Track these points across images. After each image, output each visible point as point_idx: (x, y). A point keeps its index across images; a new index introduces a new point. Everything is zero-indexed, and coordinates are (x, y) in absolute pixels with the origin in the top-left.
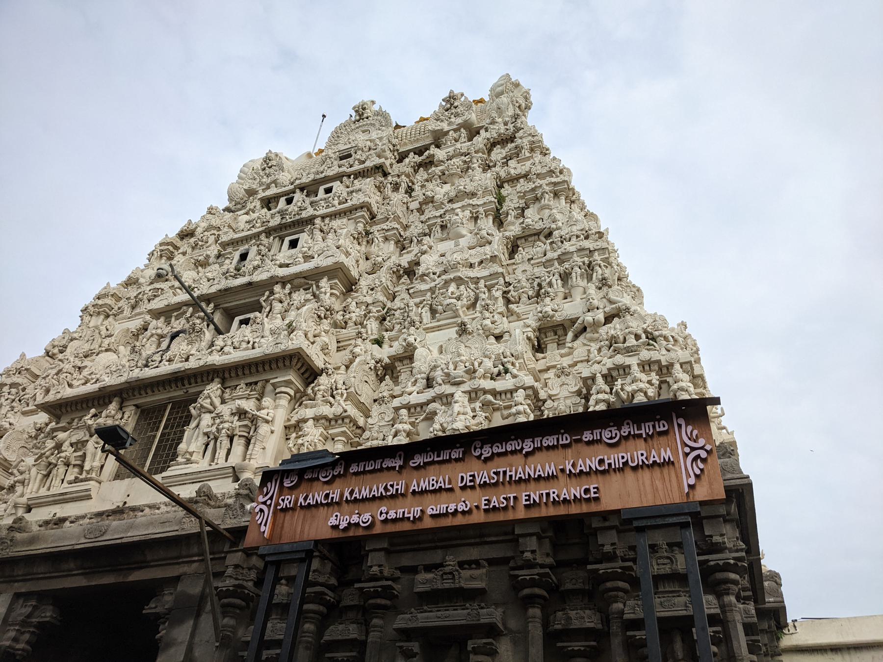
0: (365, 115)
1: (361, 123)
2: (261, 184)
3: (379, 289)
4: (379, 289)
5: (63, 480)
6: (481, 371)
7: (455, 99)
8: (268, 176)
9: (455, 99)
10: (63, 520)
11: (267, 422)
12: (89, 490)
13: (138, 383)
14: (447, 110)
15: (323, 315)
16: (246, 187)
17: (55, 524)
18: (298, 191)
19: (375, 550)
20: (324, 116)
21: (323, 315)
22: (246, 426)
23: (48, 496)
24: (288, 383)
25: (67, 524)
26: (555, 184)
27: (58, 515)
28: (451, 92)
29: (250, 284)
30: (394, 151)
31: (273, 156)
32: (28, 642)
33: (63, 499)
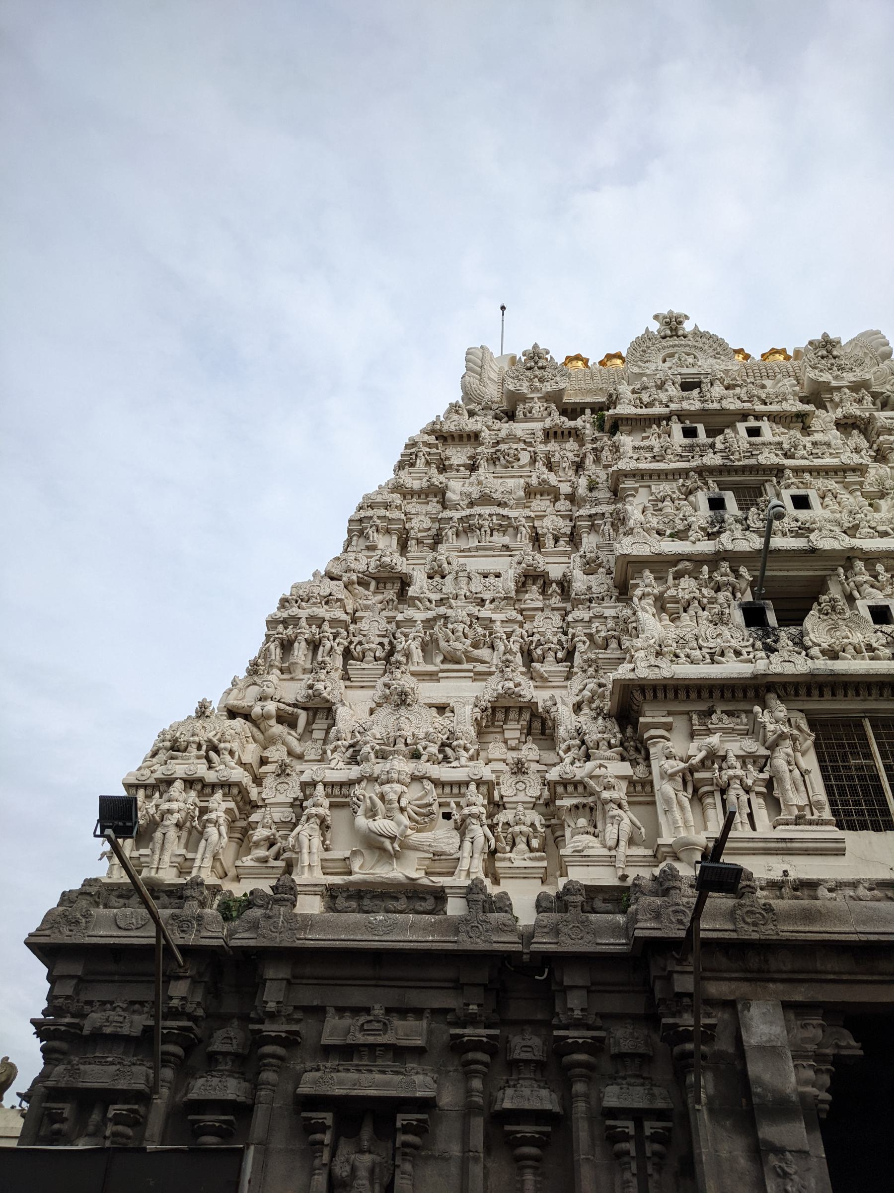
0: (680, 332)
1: (675, 341)
2: (535, 390)
5: (750, 816)
7: (834, 346)
8: (542, 380)
10: (810, 886)
12: (842, 841)
13: (830, 678)
14: (823, 357)
16: (511, 388)
17: (796, 889)
18: (674, 418)
20: (503, 308)
23: (752, 840)
25: (822, 892)
27: (793, 875)
28: (825, 335)
33: (785, 848)
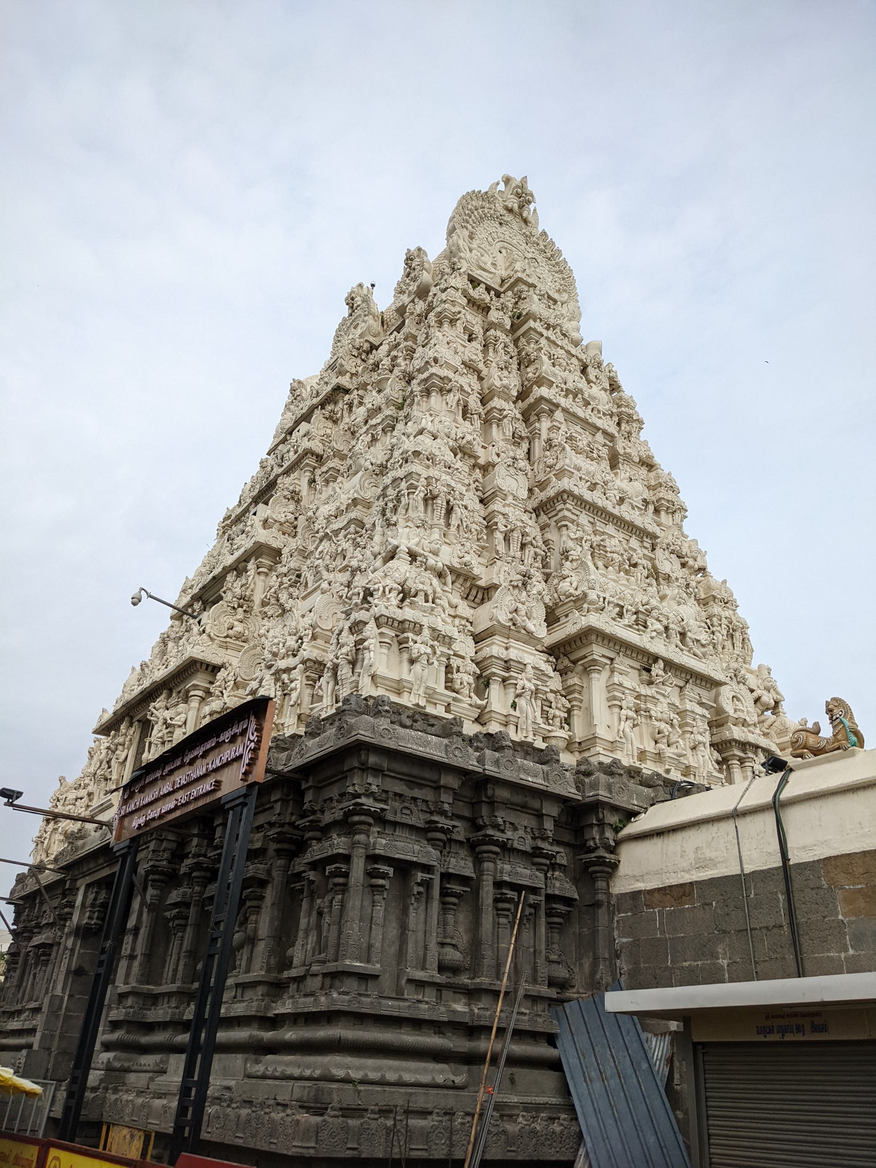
3: (296, 554)
4: (296, 554)
6: (283, 651)
7: (412, 260)
9: (412, 260)
11: (180, 726)
15: (236, 606)
19: (218, 825)
21: (236, 606)
22: (169, 732)
24: (196, 687)
26: (426, 380)
29: (214, 578)
30: (360, 354)
31: (296, 385)
32: (97, 918)
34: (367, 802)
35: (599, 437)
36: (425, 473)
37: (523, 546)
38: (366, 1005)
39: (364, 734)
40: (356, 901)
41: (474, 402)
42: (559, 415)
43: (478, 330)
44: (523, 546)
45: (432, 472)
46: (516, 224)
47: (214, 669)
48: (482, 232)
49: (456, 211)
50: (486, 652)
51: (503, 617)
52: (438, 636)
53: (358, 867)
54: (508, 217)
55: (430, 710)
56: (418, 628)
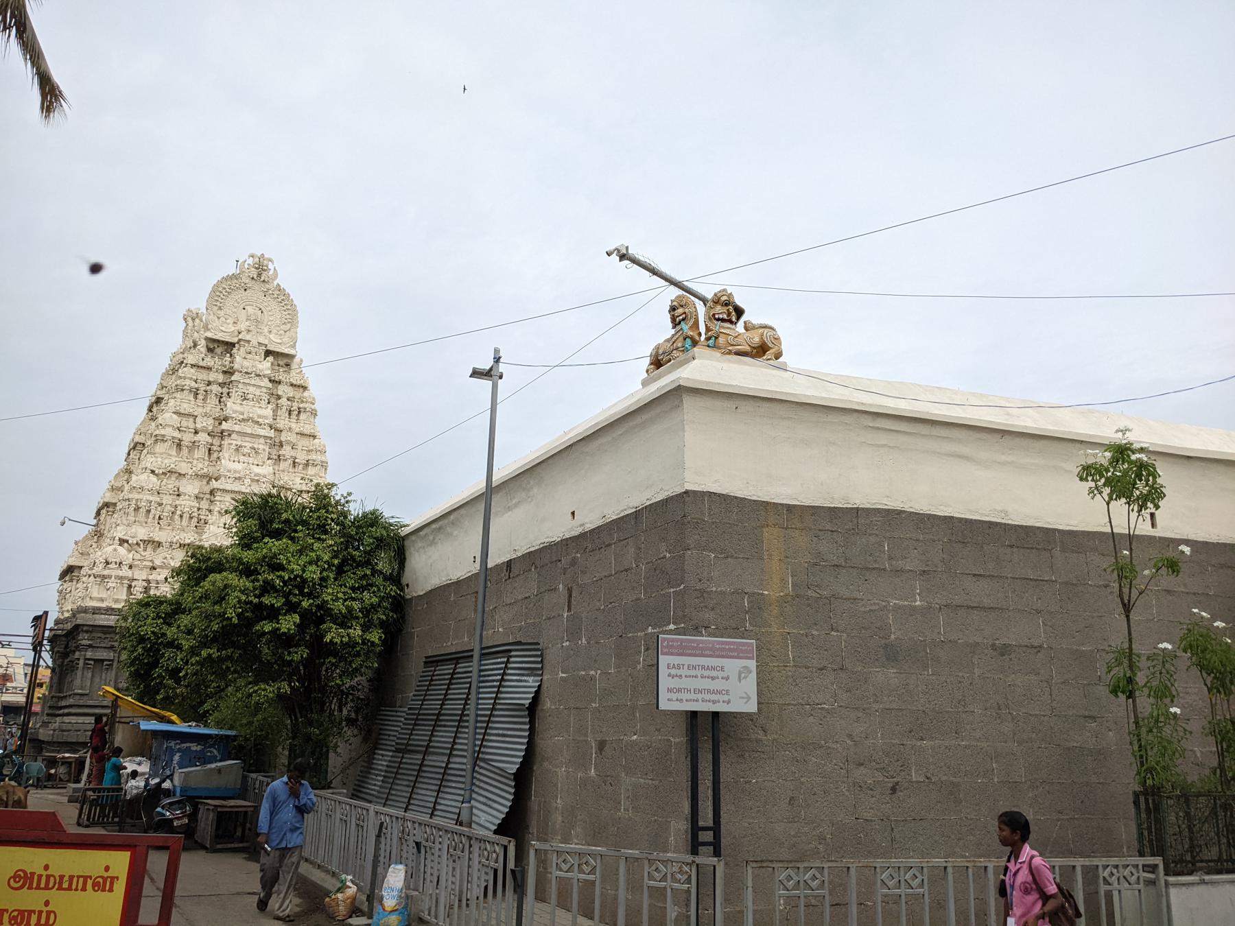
34: (84, 642)
35: (262, 441)
36: (137, 496)
37: (191, 518)
38: (81, 702)
39: (79, 622)
40: (79, 673)
41: (187, 438)
42: (234, 436)
43: (202, 387)
44: (191, 518)
45: (140, 496)
46: (257, 286)
47: (81, 568)
48: (230, 302)
49: (211, 297)
50: (151, 577)
51: (158, 562)
52: (121, 578)
53: (81, 662)
54: (250, 284)
55: (114, 606)
56: (110, 577)
